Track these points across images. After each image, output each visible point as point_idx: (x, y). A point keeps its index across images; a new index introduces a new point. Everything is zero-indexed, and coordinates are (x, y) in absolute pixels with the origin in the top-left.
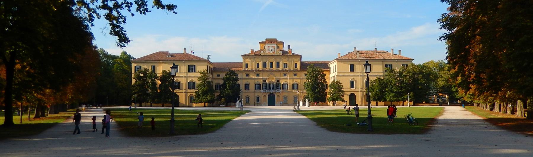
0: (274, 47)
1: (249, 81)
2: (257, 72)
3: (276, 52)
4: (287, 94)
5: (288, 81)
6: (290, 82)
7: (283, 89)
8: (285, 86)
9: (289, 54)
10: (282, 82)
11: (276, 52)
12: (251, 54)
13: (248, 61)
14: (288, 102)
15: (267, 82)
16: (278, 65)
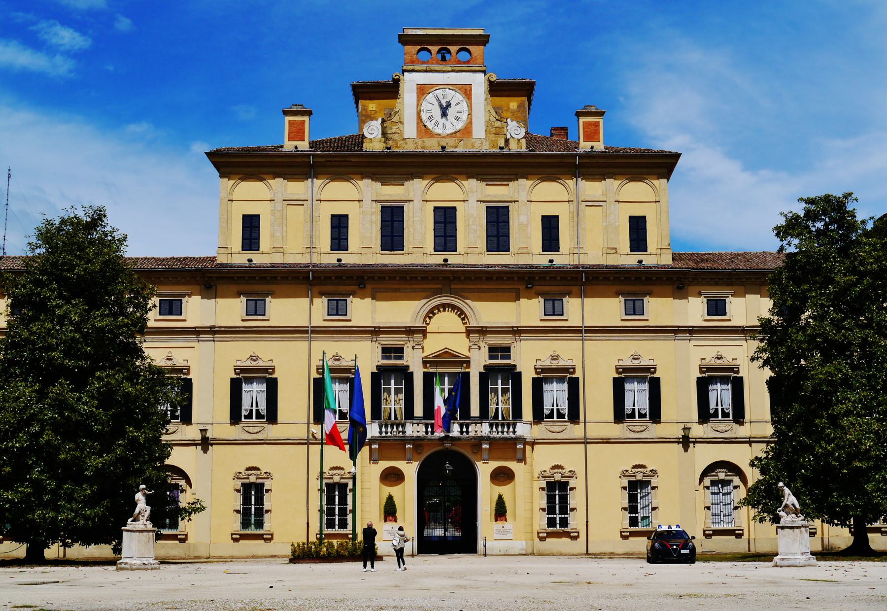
0: (466, 90)
1: (268, 352)
2: (337, 283)
3: (479, 131)
4: (569, 458)
5: (567, 352)
6: (598, 364)
7: (539, 416)
8: (556, 395)
9: (585, 146)
10: (528, 357)
11: (479, 131)
12: (289, 146)
13: (254, 195)
14: (576, 521)
15: (413, 360)
16: (498, 223)
